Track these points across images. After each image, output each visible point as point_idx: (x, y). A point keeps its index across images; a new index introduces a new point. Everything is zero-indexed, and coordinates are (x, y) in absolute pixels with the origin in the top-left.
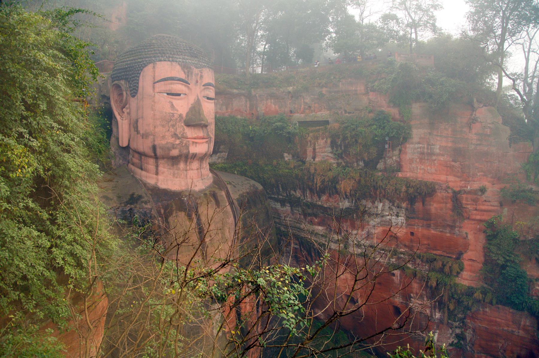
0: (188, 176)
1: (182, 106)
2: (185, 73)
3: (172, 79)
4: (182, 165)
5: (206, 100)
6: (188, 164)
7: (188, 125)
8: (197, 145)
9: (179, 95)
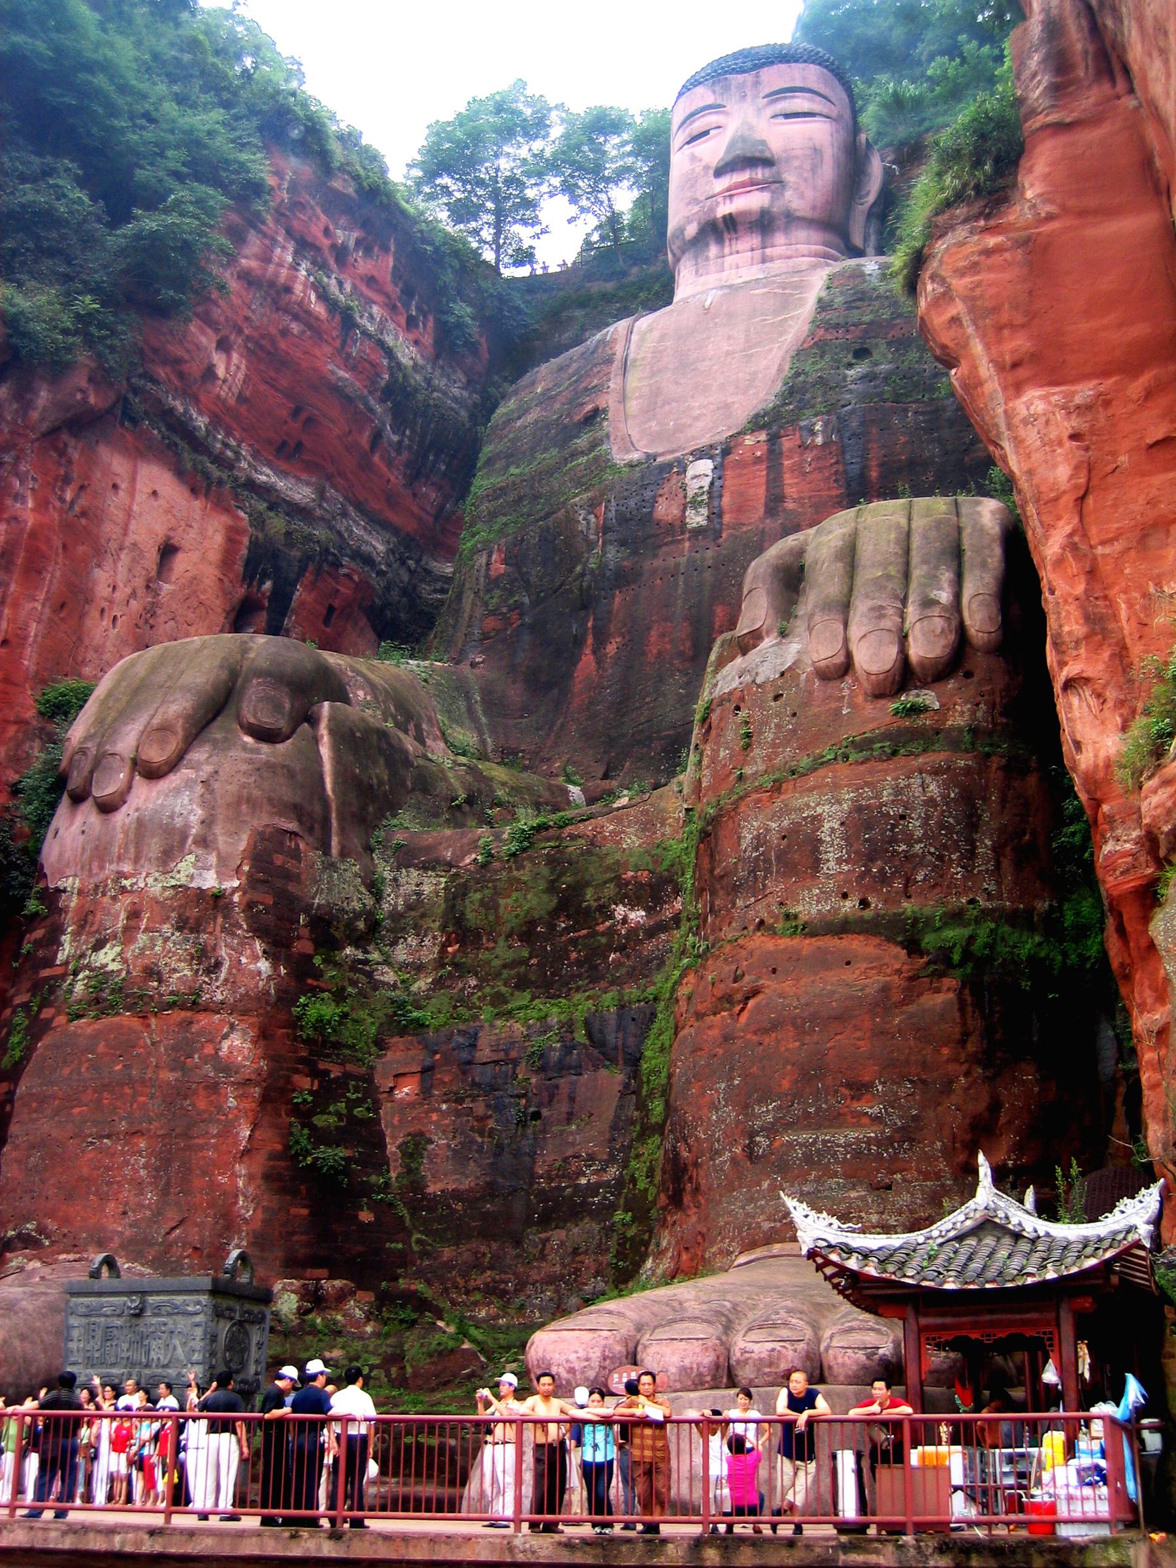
0: (726, 265)
1: (714, 150)
2: (714, 92)
3: (692, 115)
4: (713, 250)
5: (781, 120)
6: (727, 243)
7: (719, 172)
8: (735, 199)
9: (706, 133)
